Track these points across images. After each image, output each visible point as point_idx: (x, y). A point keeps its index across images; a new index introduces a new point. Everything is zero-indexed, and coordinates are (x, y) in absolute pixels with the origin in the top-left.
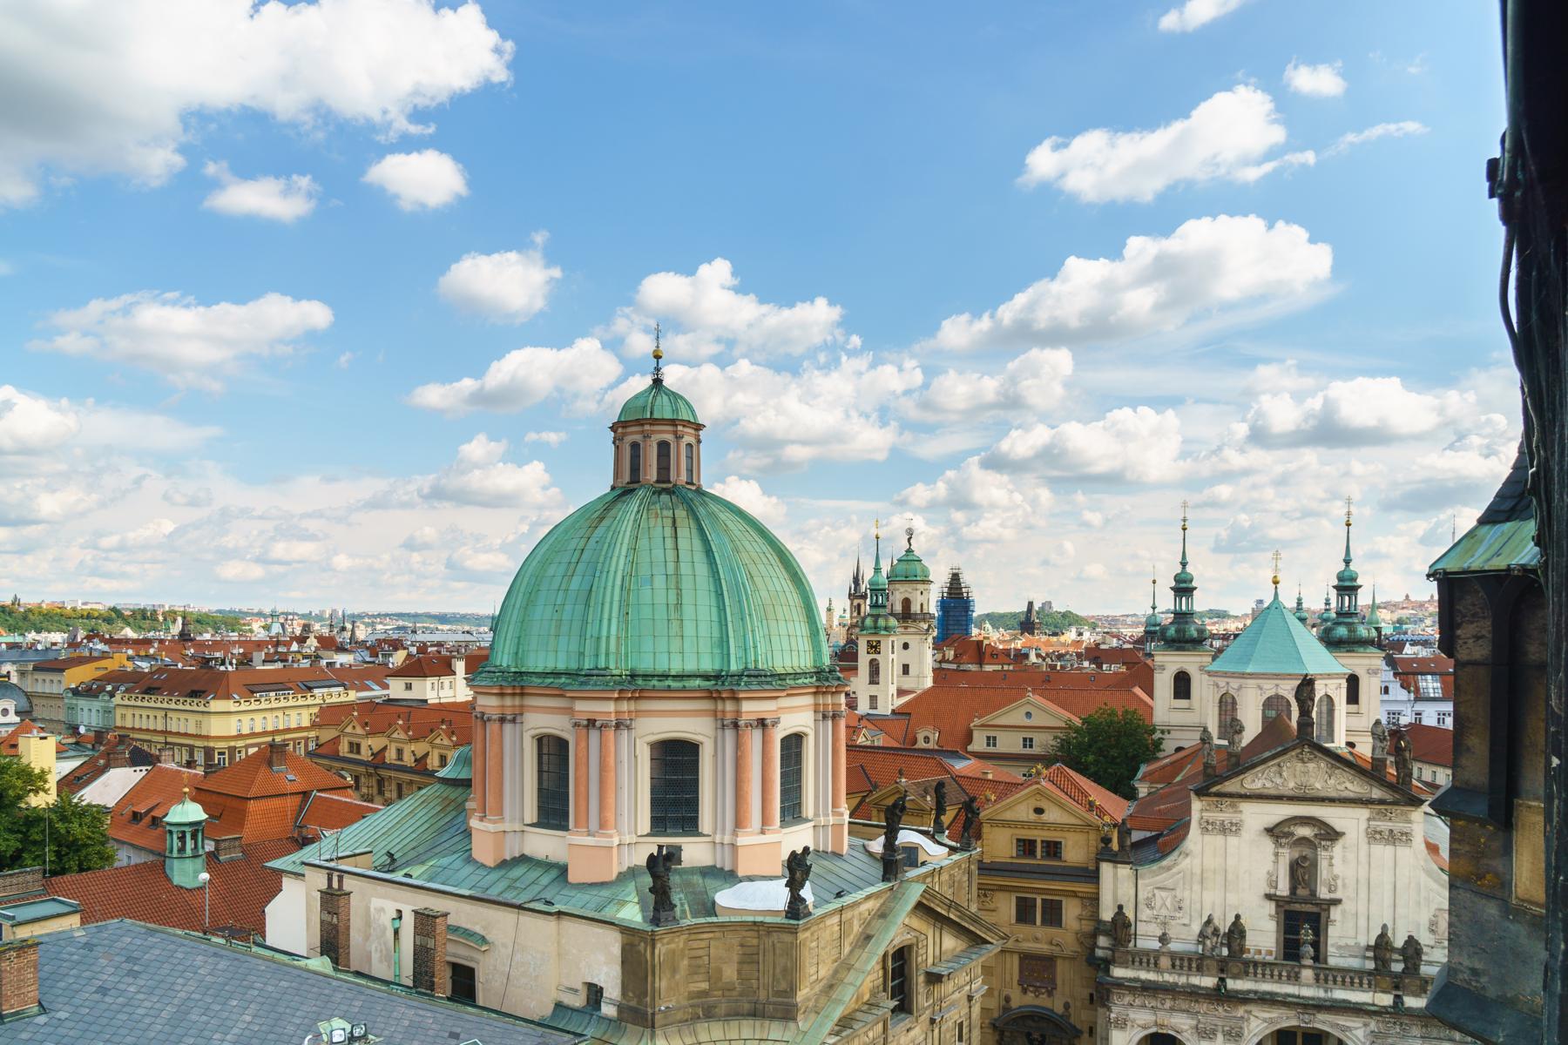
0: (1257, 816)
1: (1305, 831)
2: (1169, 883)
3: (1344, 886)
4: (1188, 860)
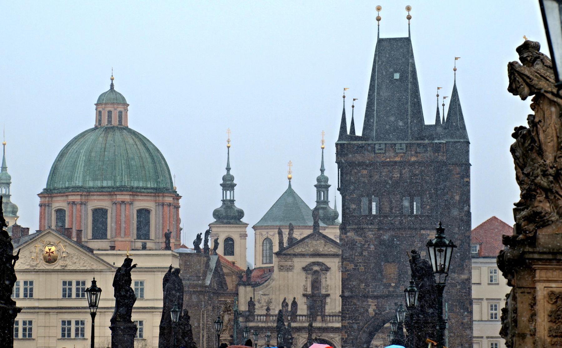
0: (299, 263)
1: (316, 268)
2: (267, 293)
3: (331, 289)
4: (274, 282)
